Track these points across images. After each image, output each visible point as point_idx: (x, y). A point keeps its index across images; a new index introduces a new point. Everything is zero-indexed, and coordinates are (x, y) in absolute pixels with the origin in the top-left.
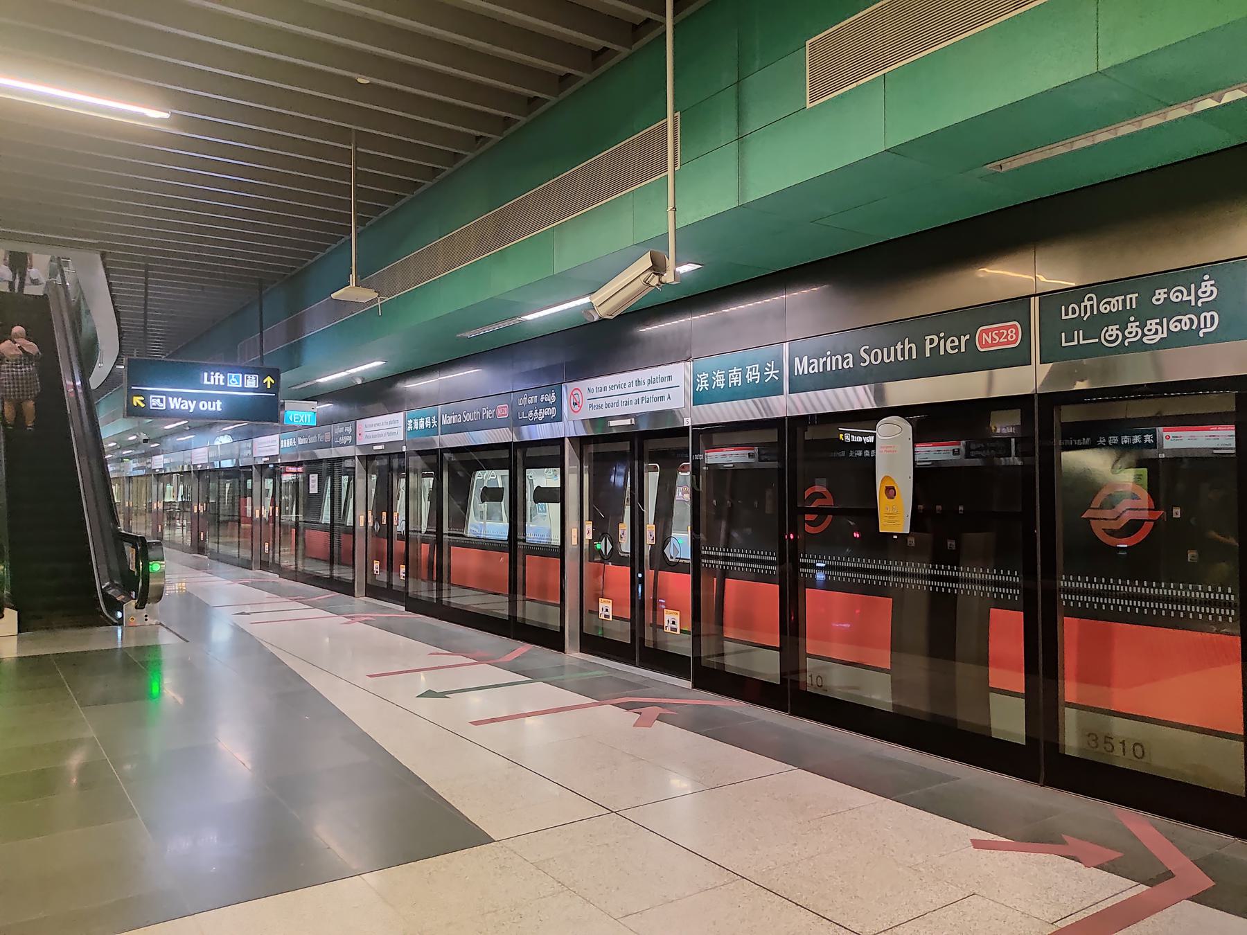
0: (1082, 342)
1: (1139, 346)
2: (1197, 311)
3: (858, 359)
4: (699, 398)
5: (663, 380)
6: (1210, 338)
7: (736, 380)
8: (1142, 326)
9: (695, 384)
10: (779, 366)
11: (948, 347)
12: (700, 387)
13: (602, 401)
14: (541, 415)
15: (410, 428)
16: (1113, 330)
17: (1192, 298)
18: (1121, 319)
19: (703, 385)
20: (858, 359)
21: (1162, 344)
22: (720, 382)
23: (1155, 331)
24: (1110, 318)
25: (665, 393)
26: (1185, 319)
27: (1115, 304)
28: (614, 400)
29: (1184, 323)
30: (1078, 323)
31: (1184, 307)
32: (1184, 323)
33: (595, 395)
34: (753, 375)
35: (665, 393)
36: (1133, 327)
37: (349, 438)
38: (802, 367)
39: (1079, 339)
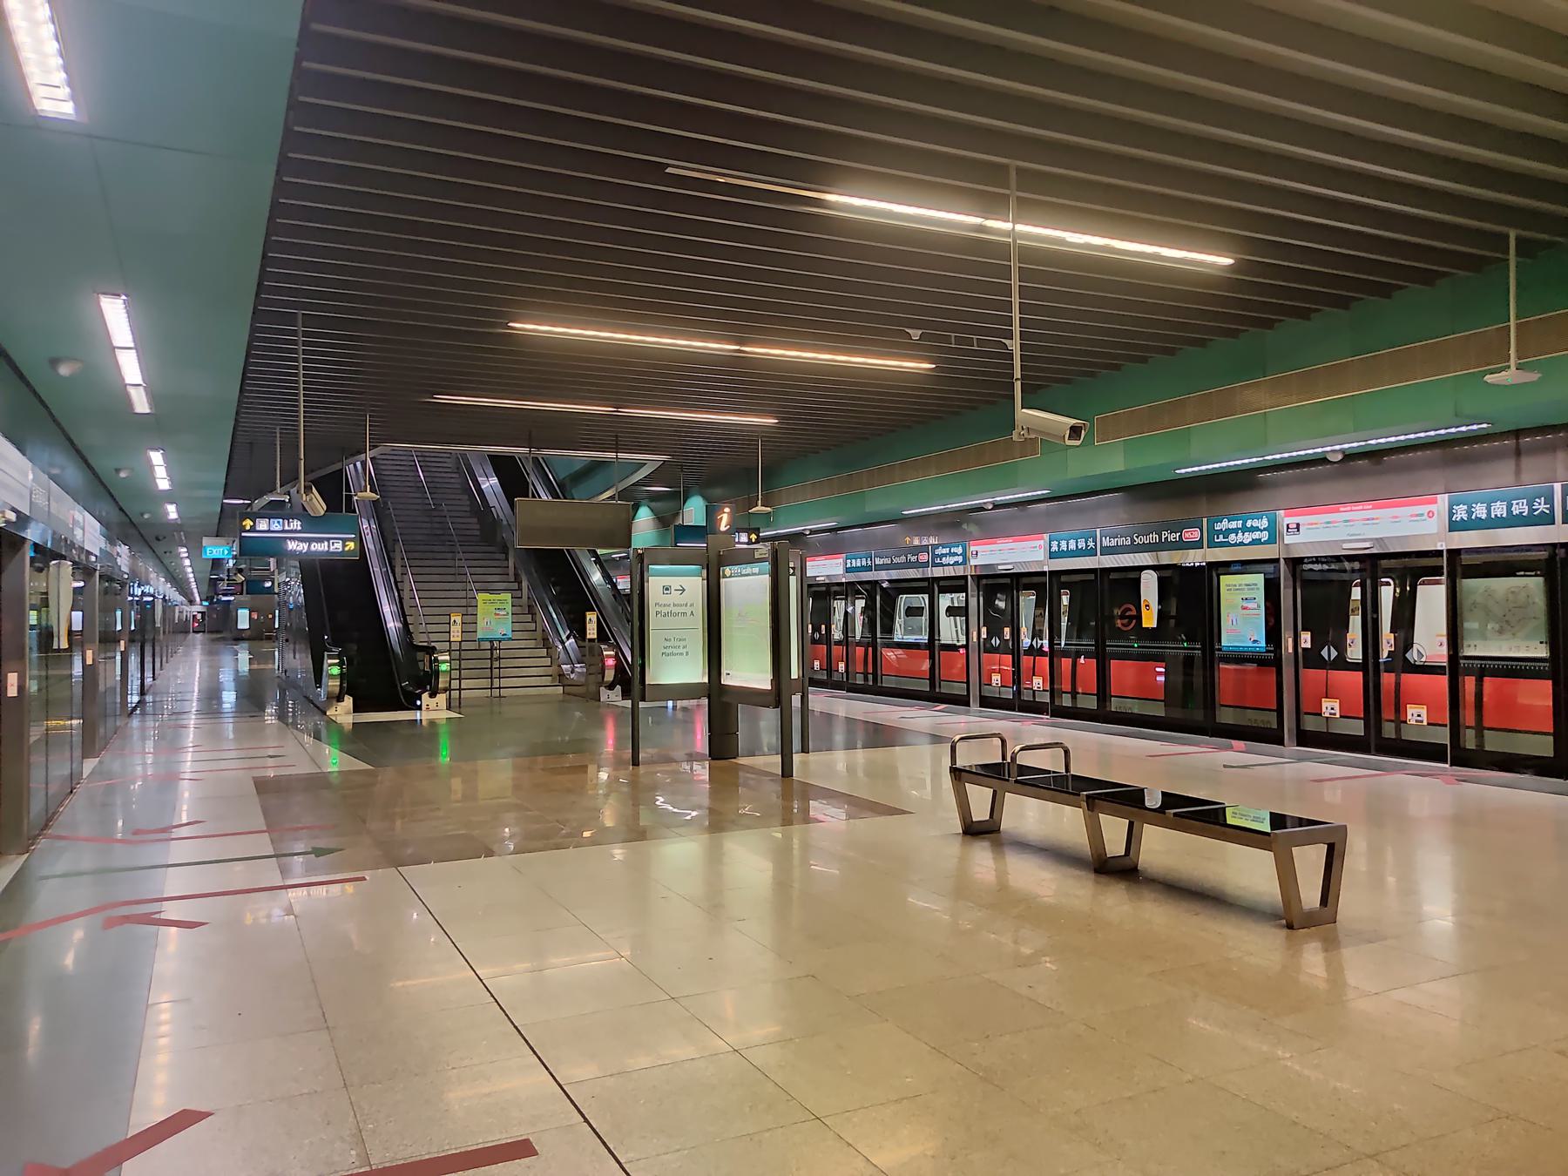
3: (1133, 541)
4: (1052, 555)
7: (1072, 546)
14: (952, 560)
20: (1133, 541)
34: (1082, 544)
38: (1106, 543)
39: (1221, 538)
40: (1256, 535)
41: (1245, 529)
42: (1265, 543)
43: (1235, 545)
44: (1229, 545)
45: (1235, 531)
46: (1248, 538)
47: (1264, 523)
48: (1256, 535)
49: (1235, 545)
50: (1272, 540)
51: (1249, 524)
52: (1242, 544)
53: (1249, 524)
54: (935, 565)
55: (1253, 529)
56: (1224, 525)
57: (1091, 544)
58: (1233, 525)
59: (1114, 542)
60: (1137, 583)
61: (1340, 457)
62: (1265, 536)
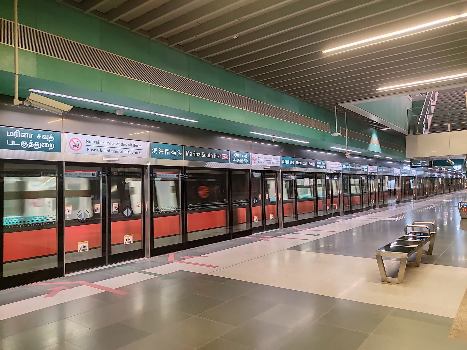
0: (14, 144)
2: (49, 143)
5: (136, 146)
8: (34, 143)
9: (151, 151)
10: (182, 152)
11: (218, 156)
13: (99, 148)
15: (283, 163)
16: (25, 143)
17: (48, 139)
18: (28, 140)
19: (155, 151)
22: (161, 151)
23: (37, 146)
24: (24, 139)
25: (138, 151)
26: (46, 144)
28: (265, 161)
30: (13, 138)
31: (46, 141)
32: (45, 145)
33: (92, 144)
35: (138, 151)
36: (31, 143)
37: (324, 167)
40: (245, 160)
41: (35, 140)
42: (52, 151)
43: (27, 149)
44: (236, 162)
45: (239, 158)
47: (246, 157)
48: (245, 160)
52: (241, 163)
53: (39, 136)
54: (318, 168)
55: (41, 141)
58: (25, 135)
59: (192, 154)
61: (68, 108)
62: (247, 161)
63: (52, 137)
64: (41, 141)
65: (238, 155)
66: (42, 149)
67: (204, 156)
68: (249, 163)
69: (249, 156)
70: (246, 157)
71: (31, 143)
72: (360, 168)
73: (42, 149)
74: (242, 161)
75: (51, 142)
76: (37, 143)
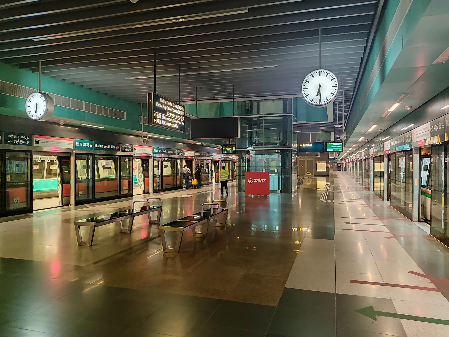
1: (19, 144)
2: (27, 140)
6: (28, 145)
12: (77, 145)
16: (16, 141)
18: (17, 139)
21: (22, 144)
23: (21, 142)
27: (16, 137)
29: (25, 142)
32: (25, 142)
36: (18, 141)
40: (130, 150)
41: (20, 139)
42: (28, 145)
43: (17, 144)
45: (126, 148)
46: (128, 150)
47: (131, 147)
48: (130, 150)
49: (17, 144)
50: (132, 151)
51: (22, 137)
56: (124, 146)
57: (91, 146)
58: (16, 137)
59: (98, 146)
60: (69, 158)
63: (28, 137)
64: (23, 139)
65: (126, 146)
66: (24, 144)
67: (105, 147)
68: (132, 151)
69: (132, 147)
70: (131, 147)
71: (18, 141)
72: (208, 155)
73: (24, 144)
74: (128, 150)
75: (28, 140)
76: (21, 141)
